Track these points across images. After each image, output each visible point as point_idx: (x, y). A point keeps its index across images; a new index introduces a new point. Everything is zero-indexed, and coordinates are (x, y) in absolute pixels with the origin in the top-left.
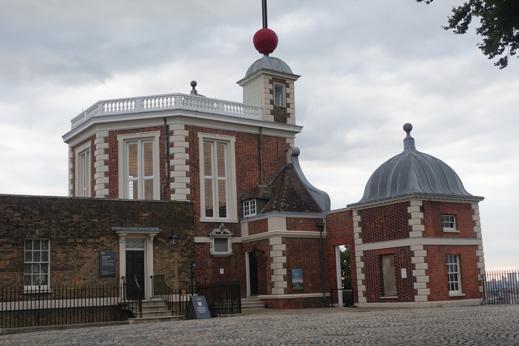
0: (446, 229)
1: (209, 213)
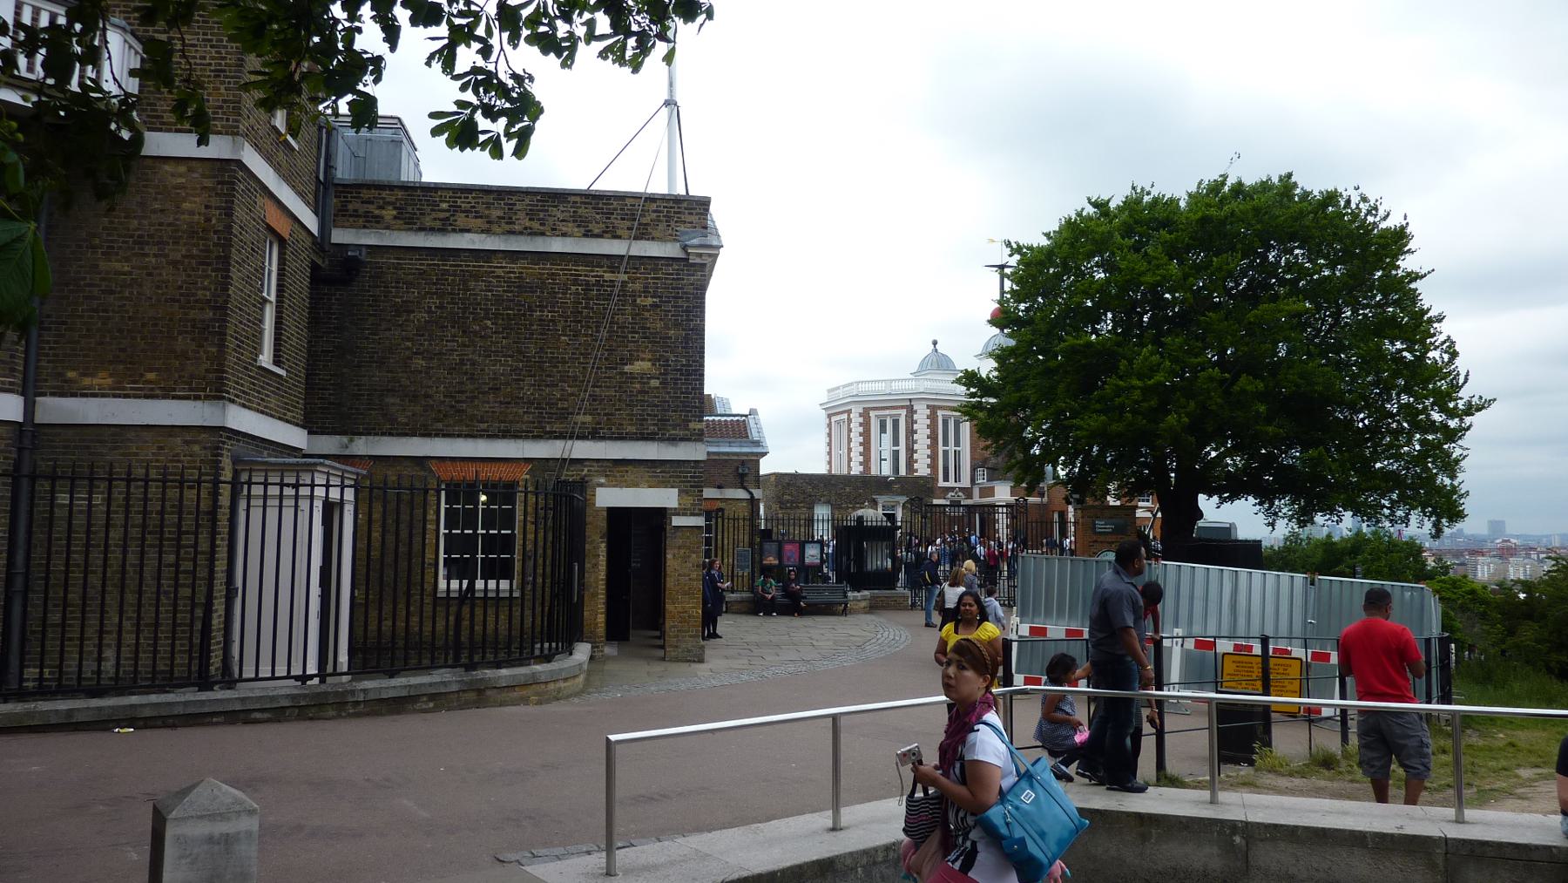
1: (946, 479)
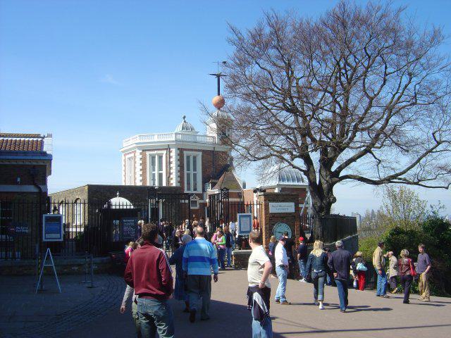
1: (189, 189)
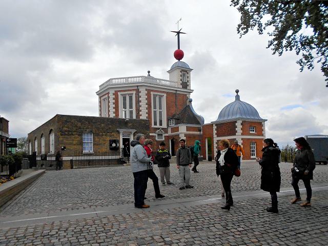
0: (251, 132)
1: (155, 124)
